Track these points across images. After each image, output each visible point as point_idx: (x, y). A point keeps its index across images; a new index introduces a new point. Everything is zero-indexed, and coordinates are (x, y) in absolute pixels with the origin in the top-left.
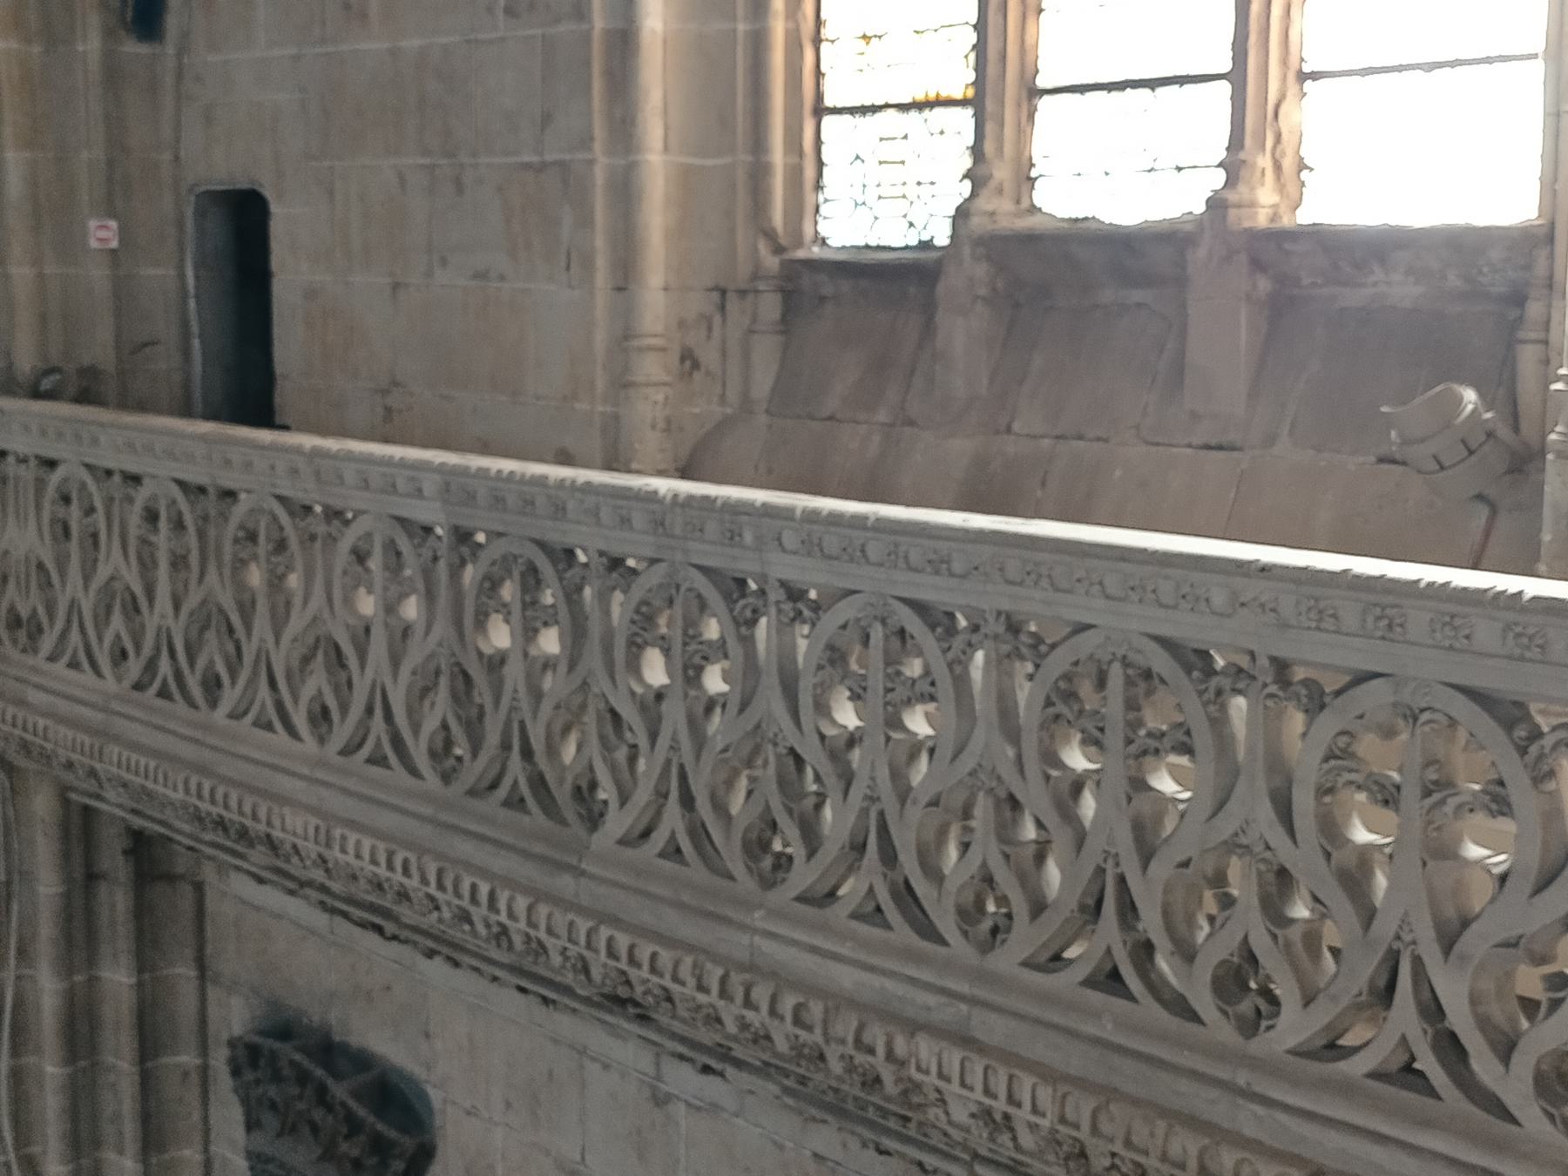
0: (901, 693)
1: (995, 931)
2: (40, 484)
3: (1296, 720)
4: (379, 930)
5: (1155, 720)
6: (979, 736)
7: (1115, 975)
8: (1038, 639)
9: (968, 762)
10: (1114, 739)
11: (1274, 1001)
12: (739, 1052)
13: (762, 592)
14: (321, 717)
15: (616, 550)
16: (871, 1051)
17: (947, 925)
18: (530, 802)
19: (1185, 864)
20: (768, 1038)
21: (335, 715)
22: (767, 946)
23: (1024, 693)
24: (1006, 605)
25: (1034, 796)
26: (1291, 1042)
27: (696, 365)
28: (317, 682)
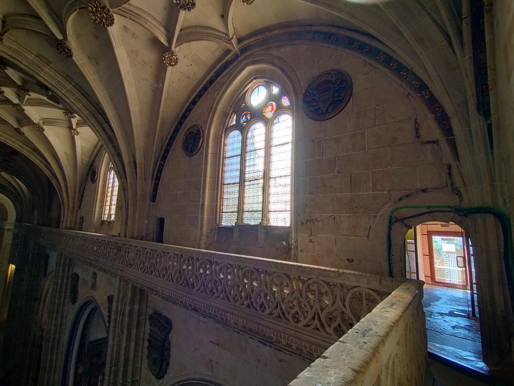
0: (228, 274)
1: (237, 301)
2: (135, 249)
3: (268, 277)
4: (168, 301)
5: (254, 277)
6: (236, 278)
7: (249, 306)
8: (242, 268)
9: (234, 281)
10: (249, 279)
11: (265, 308)
12: (208, 315)
13: (213, 262)
14: (164, 276)
15: (198, 258)
16: (223, 315)
17: (231, 300)
18: (187, 286)
19: (256, 293)
20: (211, 314)
21: (165, 276)
22: (212, 303)
23: (240, 273)
24: (238, 264)
25: (241, 285)
26: (267, 313)
27: (208, 237)
28: (164, 272)
